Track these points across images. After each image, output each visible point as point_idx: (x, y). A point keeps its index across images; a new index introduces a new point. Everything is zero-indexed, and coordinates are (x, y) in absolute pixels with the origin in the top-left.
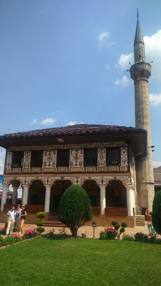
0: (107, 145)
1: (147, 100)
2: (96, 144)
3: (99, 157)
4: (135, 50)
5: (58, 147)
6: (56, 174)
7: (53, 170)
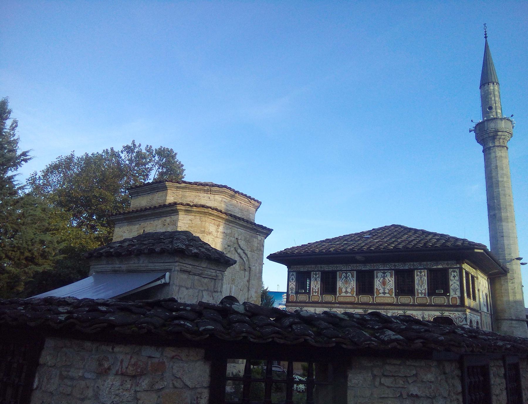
1: (505, 179)
2: (412, 263)
4: (482, 96)
7: (351, 300)
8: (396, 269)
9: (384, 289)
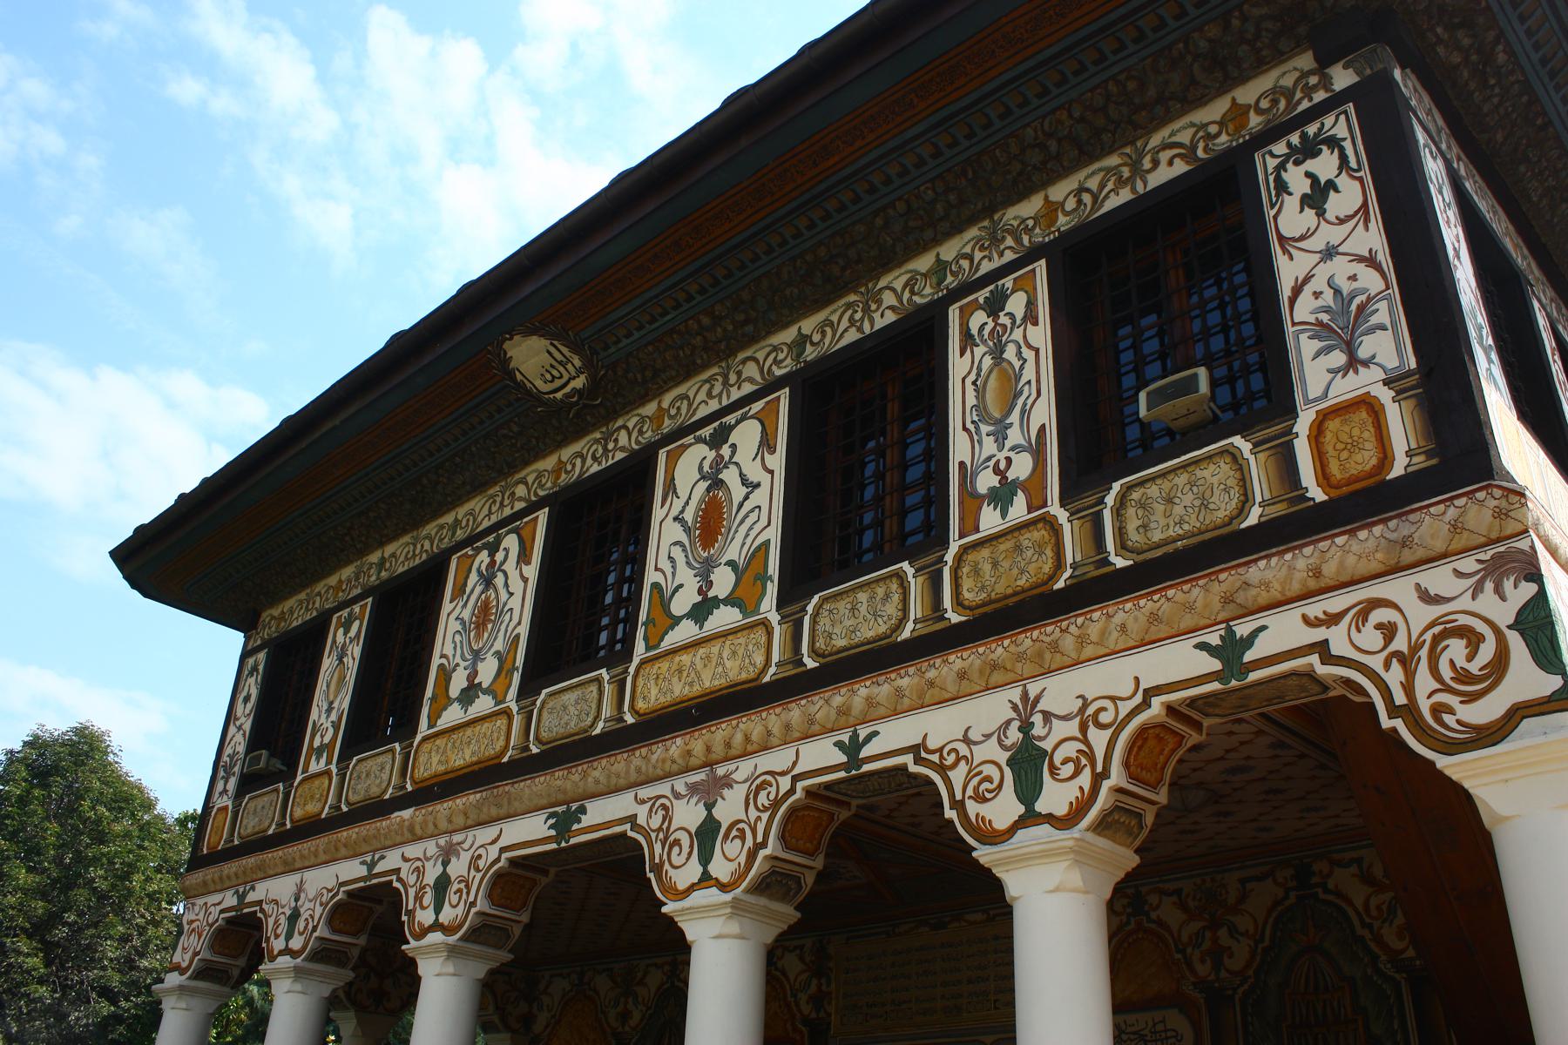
0: (1052, 209)
3: (971, 400)
9: (705, 573)
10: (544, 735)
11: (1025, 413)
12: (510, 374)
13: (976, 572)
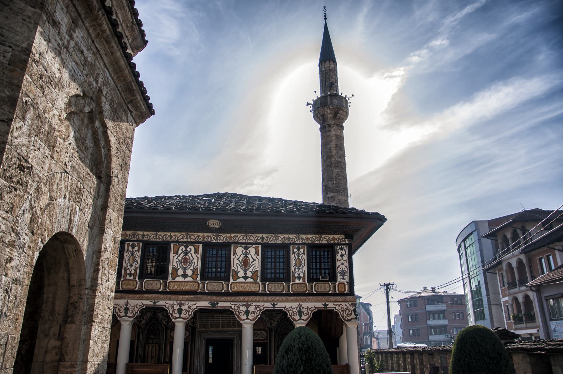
0: (308, 239)
2: (287, 236)
5: (204, 237)
6: (200, 296)
7: (194, 287)
8: (265, 243)
9: (245, 271)
10: (209, 289)
11: (302, 268)
12: (206, 222)
13: (295, 287)
